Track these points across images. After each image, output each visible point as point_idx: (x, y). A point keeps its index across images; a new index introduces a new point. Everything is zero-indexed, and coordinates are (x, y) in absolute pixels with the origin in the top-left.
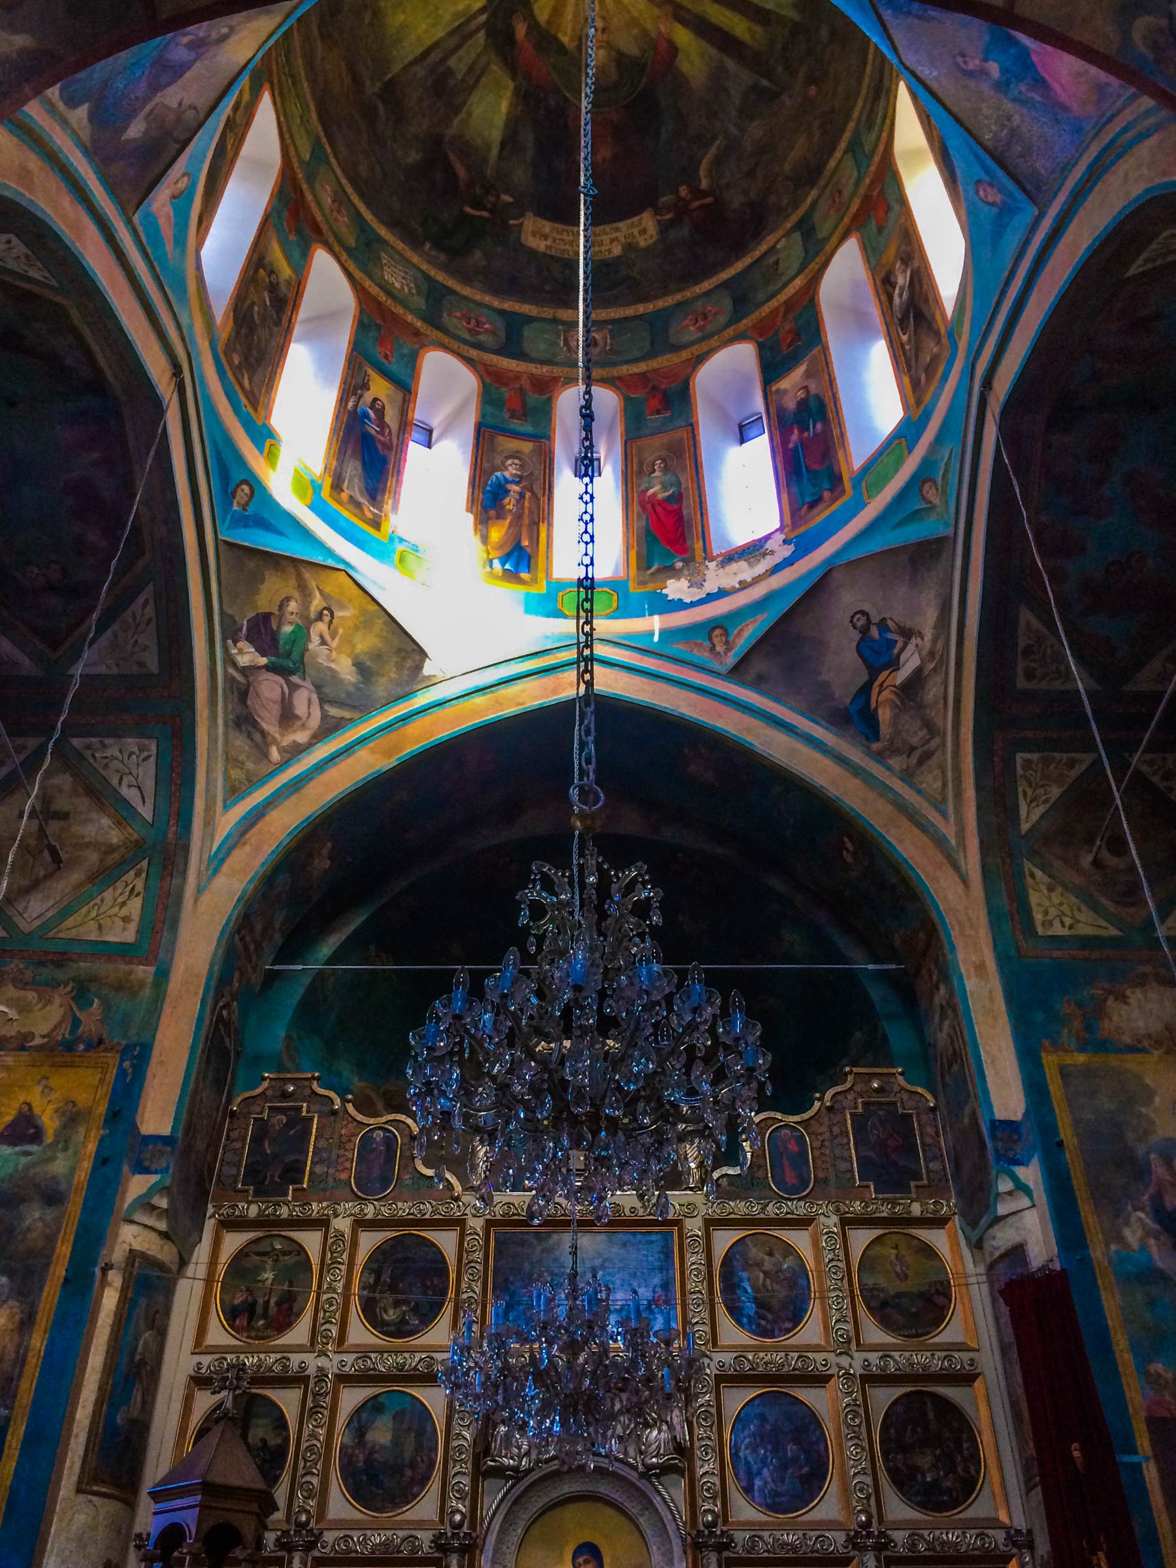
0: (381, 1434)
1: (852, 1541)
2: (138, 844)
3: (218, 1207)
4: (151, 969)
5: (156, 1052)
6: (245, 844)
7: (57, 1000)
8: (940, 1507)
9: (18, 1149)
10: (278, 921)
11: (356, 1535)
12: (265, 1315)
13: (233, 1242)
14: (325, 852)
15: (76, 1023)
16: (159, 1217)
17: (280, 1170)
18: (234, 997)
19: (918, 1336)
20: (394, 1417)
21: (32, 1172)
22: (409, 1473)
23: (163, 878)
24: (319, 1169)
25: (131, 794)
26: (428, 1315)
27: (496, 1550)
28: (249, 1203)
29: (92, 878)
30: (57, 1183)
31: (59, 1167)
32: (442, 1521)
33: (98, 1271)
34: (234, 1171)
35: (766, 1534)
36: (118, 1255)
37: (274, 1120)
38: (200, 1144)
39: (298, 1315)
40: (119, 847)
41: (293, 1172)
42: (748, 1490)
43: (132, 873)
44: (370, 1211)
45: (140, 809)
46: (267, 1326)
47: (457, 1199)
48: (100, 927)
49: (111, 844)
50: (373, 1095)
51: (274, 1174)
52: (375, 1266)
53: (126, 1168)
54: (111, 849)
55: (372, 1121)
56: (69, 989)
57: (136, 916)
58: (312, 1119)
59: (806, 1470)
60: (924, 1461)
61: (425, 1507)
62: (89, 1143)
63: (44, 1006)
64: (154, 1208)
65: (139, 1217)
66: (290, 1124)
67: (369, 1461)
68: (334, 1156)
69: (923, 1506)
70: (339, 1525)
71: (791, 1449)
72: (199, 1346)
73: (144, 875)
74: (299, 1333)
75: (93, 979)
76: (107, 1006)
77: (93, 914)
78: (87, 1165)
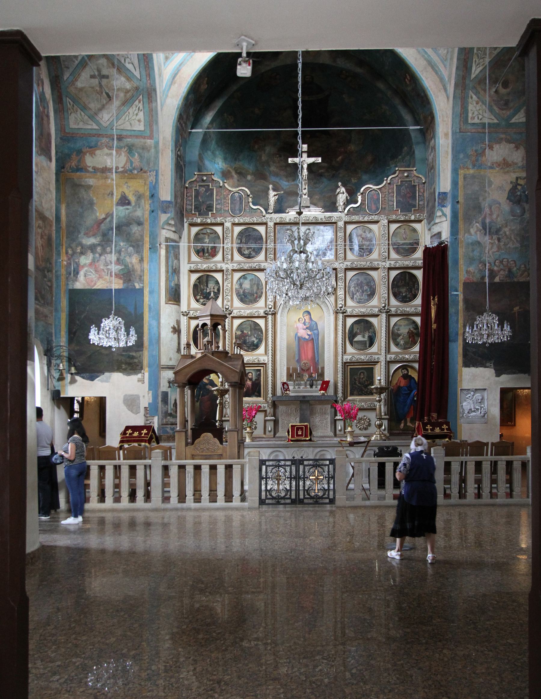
0: (247, 285)
1: (380, 311)
2: (137, 89)
3: (188, 219)
4: (152, 141)
5: (160, 172)
6: (175, 83)
7: (123, 154)
8: (405, 302)
9: (124, 207)
10: (191, 111)
11: (242, 311)
12: (208, 252)
13: (195, 230)
14: (205, 82)
15: (132, 163)
16: (172, 227)
17: (205, 207)
18: (181, 146)
19: (407, 256)
20: (250, 280)
21: (131, 215)
22: (255, 295)
23: (149, 104)
24: (218, 207)
25: (130, 67)
26: (258, 251)
27: (281, 313)
28: (197, 218)
29: (123, 104)
30: (140, 219)
31: (139, 213)
32: (266, 307)
33: (158, 245)
34: (190, 207)
35: (356, 309)
36: (162, 239)
37: (201, 190)
38: (179, 201)
39: (218, 252)
40: (130, 90)
41: (210, 208)
42: (352, 298)
43: (137, 101)
44: (236, 221)
45: (135, 73)
46: (209, 255)
47: (264, 216)
48: (131, 124)
49: (127, 89)
50: (231, 170)
51: (204, 208)
52: (240, 237)
53: (159, 212)
54: (127, 91)
55: (234, 190)
56: (126, 149)
57: (142, 119)
58: (213, 189)
59: (369, 293)
60: (403, 290)
61: (261, 303)
62: (147, 205)
63: (119, 156)
64: (170, 224)
65: (166, 227)
66: (206, 191)
67: (244, 292)
68: (222, 202)
69: (401, 302)
70: (237, 308)
71: (366, 287)
72: (189, 262)
73: (142, 102)
74: (219, 257)
75: (133, 145)
76: (141, 156)
77: (127, 119)
78: (147, 213)
